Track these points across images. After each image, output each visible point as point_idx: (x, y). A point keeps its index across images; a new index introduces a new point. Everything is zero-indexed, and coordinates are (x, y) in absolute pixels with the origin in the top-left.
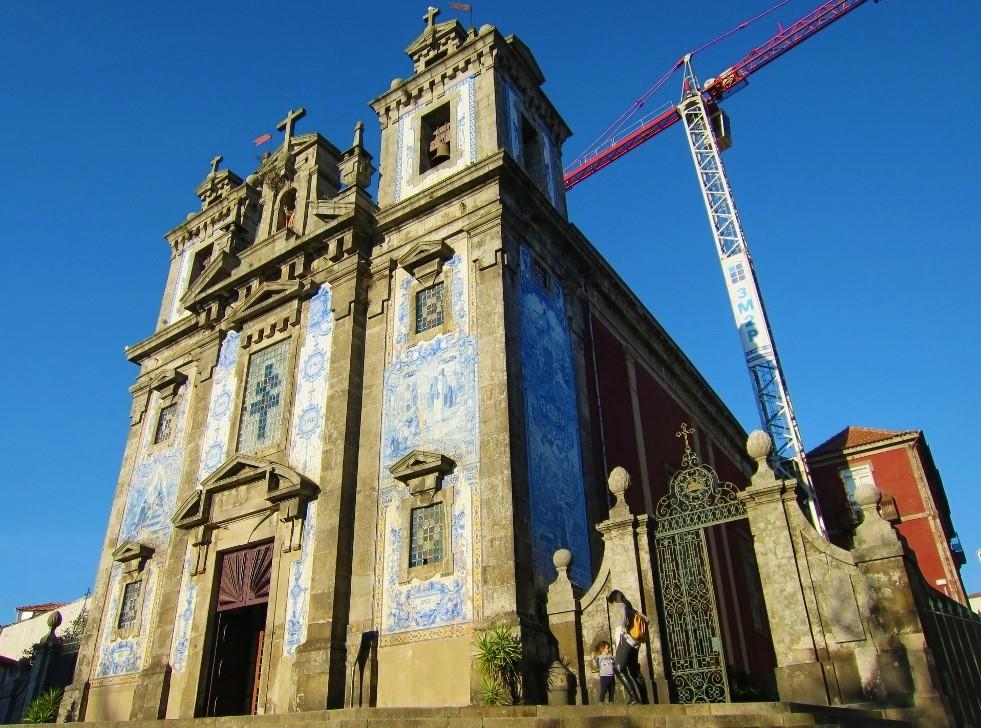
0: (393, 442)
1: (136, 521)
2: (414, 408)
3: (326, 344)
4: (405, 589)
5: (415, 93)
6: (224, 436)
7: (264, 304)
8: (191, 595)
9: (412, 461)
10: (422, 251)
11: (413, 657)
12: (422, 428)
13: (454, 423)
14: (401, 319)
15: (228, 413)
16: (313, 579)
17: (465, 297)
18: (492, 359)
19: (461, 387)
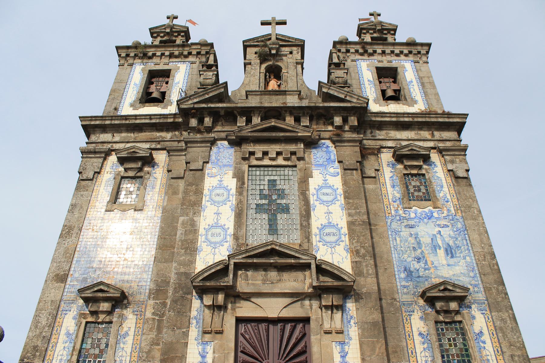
0: (405, 270)
2: (419, 251)
3: (337, 182)
5: (370, 51)
7: (274, 134)
8: (204, 350)
9: (442, 288)
12: (430, 266)
14: (393, 186)
15: (229, 204)
17: (446, 189)
18: (480, 235)
19: (458, 247)
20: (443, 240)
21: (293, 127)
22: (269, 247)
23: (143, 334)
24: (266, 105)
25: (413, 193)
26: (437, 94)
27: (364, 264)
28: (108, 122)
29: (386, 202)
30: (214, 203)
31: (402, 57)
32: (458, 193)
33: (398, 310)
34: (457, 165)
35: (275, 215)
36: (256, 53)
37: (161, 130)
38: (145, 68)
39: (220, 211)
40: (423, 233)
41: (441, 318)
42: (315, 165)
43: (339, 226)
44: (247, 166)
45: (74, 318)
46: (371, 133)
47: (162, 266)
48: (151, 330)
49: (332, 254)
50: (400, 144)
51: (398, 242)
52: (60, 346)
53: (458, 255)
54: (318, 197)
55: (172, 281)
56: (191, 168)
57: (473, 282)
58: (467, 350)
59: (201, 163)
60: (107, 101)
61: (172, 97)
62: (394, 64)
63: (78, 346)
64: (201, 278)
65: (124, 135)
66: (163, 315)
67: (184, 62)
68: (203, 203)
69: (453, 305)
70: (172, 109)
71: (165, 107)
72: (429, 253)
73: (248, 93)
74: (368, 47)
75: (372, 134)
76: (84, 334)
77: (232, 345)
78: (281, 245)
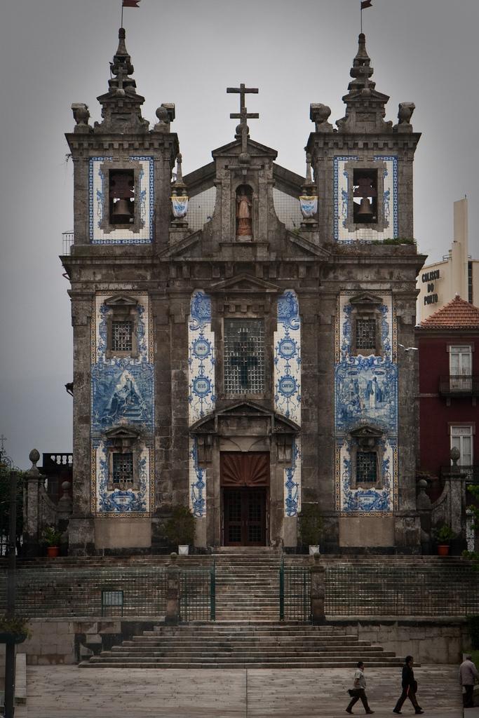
0: (343, 411)
1: (109, 407)
2: (356, 396)
3: (296, 335)
4: (354, 492)
5: (351, 144)
6: (210, 372)
8: (200, 474)
10: (367, 299)
11: (360, 523)
13: (382, 412)
14: (345, 334)
16: (302, 481)
17: (390, 336)
18: (407, 382)
19: (387, 393)
20: (377, 386)
21: (262, 283)
22: (243, 403)
23: (155, 461)
24: (238, 259)
25: (361, 340)
26: (410, 213)
27: (310, 412)
28: (89, 262)
29: (337, 350)
30: (198, 356)
31: (385, 153)
32: (400, 340)
33: (333, 443)
34: (406, 311)
35: (246, 369)
36: (226, 167)
37: (141, 268)
38: (103, 165)
39: (204, 364)
40: (362, 379)
41: (362, 450)
42: (281, 318)
43: (295, 379)
44: (222, 319)
45: (103, 451)
46: (334, 273)
47: (162, 408)
48: (161, 458)
49: (288, 402)
50: (359, 286)
51: (341, 387)
52: (99, 471)
53: (385, 400)
54: (280, 351)
55: (173, 425)
56: (176, 322)
57: (392, 423)
58: (375, 472)
59: (184, 316)
60: (75, 220)
61: (142, 215)
62: (375, 164)
63: (112, 471)
64: (196, 428)
65: (104, 272)
66: (168, 447)
67: (145, 157)
68: (189, 356)
69: (371, 442)
70: (144, 234)
71: (136, 231)
72: (363, 398)
73: (221, 245)
74: (349, 139)
75: (335, 274)
76: (114, 462)
77: (218, 471)
78: (250, 403)
